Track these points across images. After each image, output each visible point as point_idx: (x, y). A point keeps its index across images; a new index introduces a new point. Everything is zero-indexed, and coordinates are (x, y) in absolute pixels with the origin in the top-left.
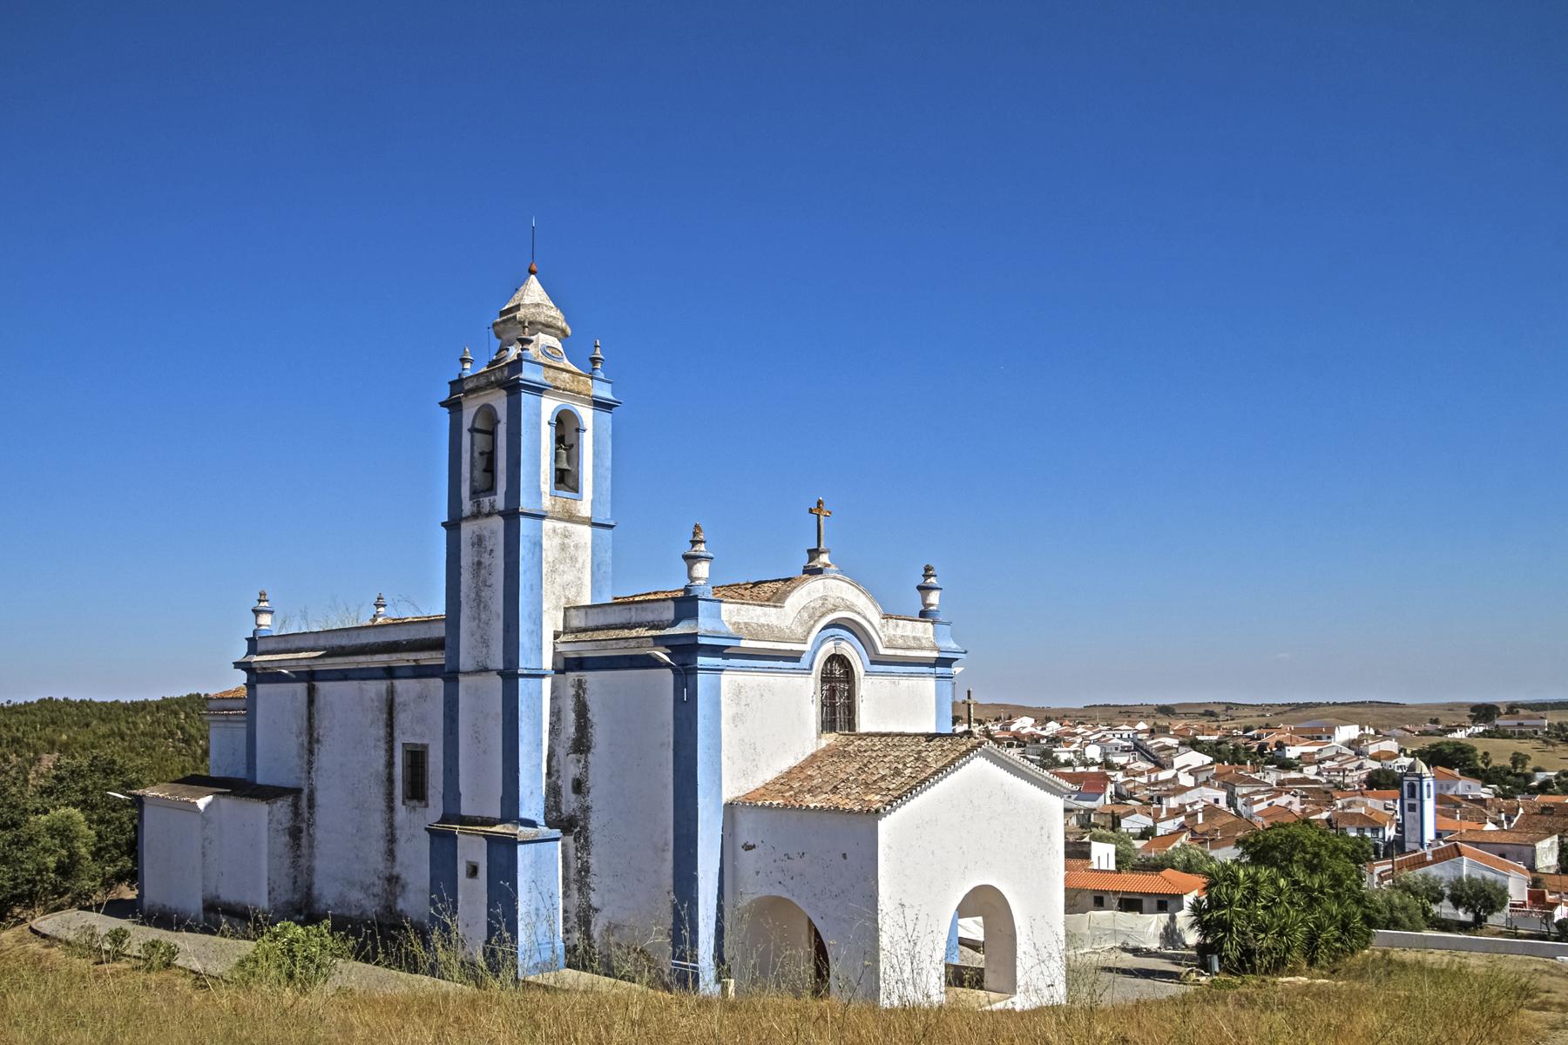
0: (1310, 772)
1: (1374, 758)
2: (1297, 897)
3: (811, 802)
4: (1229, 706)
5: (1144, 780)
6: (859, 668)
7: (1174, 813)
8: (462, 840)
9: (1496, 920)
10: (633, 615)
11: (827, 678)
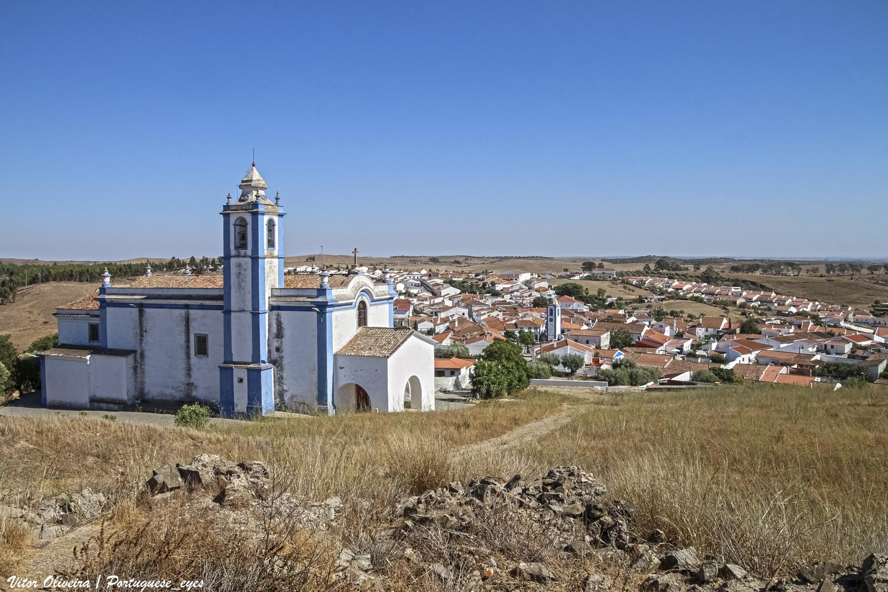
0: (507, 298)
1: (537, 291)
2: (504, 371)
3: (366, 353)
4: (467, 258)
5: (427, 303)
6: (368, 304)
7: (444, 321)
8: (235, 370)
9: (580, 371)
10: (300, 293)
11: (359, 309)
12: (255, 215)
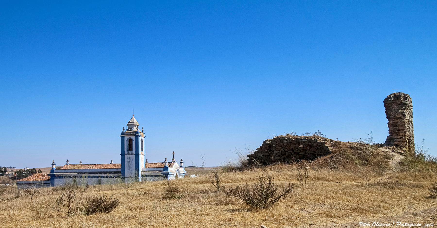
10: (156, 169)
12: (137, 137)
